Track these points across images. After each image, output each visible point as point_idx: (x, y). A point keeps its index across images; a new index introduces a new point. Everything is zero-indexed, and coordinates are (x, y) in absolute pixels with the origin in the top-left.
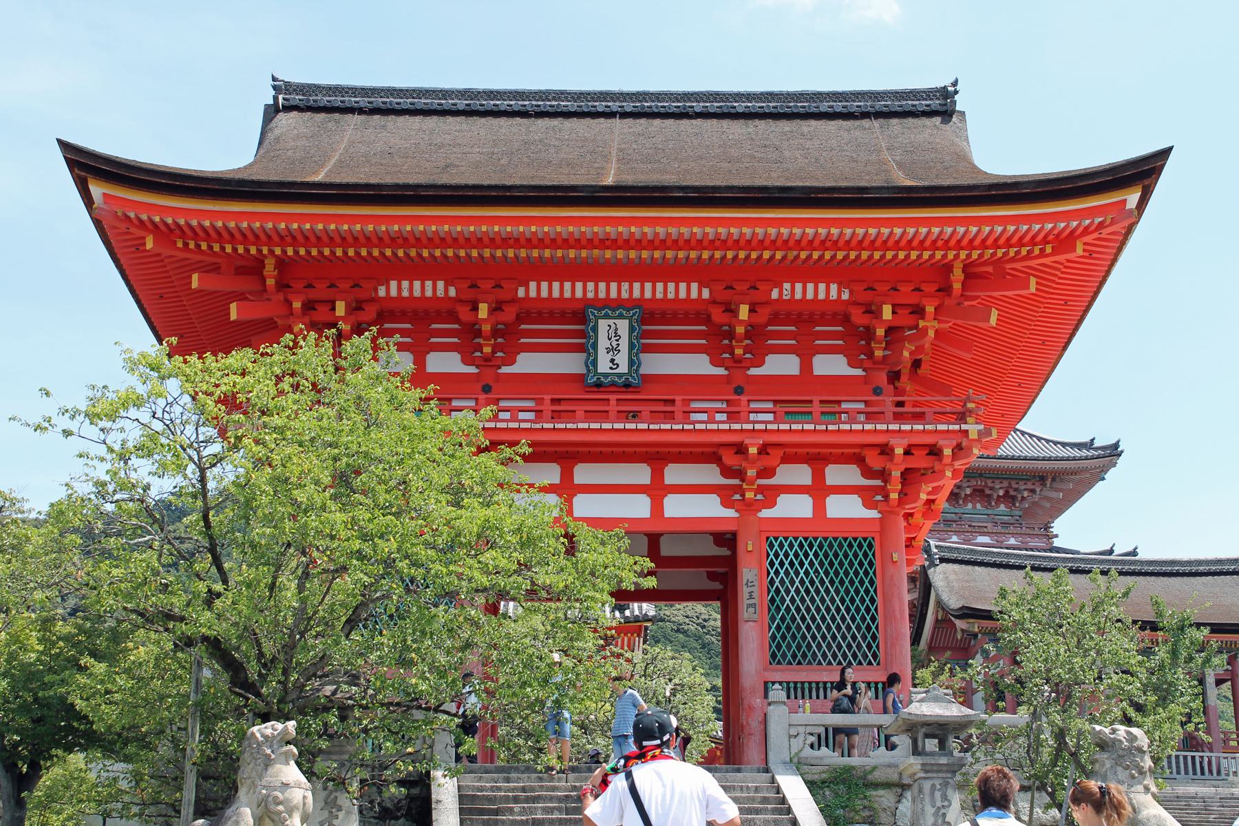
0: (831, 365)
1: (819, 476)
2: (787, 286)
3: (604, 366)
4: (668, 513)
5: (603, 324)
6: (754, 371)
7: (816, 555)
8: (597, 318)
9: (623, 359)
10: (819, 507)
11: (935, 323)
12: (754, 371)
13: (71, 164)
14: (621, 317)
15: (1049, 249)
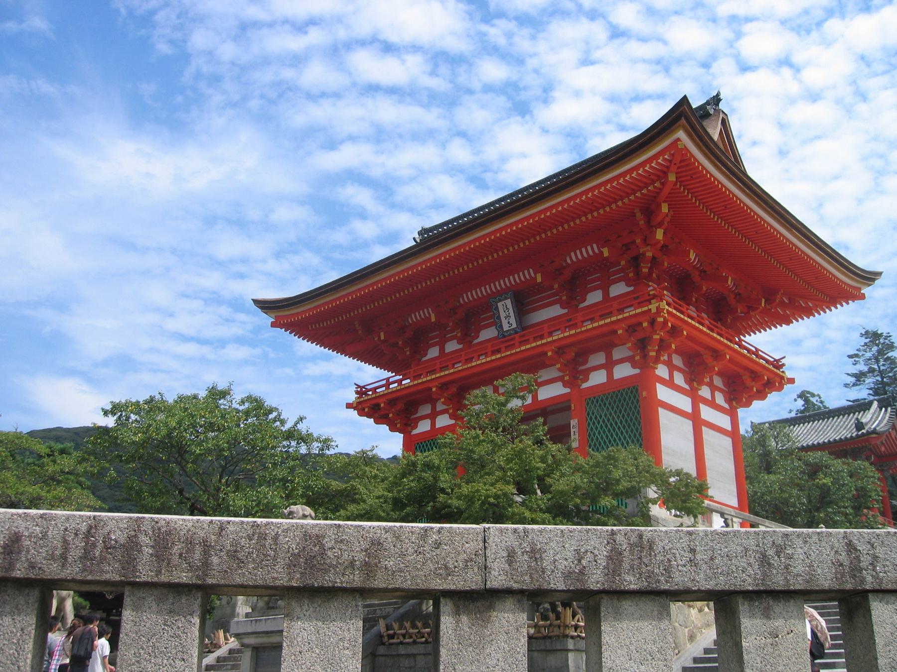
0: (618, 289)
1: (609, 356)
2: (573, 254)
3: (506, 327)
4: (540, 398)
5: (500, 305)
6: (582, 305)
7: (610, 404)
8: (496, 303)
9: (513, 320)
10: (610, 375)
11: (649, 248)
12: (582, 305)
13: (262, 308)
14: (506, 298)
15: (657, 184)
